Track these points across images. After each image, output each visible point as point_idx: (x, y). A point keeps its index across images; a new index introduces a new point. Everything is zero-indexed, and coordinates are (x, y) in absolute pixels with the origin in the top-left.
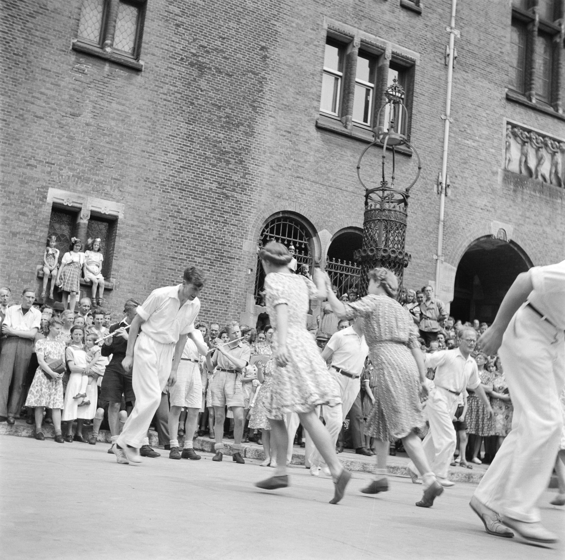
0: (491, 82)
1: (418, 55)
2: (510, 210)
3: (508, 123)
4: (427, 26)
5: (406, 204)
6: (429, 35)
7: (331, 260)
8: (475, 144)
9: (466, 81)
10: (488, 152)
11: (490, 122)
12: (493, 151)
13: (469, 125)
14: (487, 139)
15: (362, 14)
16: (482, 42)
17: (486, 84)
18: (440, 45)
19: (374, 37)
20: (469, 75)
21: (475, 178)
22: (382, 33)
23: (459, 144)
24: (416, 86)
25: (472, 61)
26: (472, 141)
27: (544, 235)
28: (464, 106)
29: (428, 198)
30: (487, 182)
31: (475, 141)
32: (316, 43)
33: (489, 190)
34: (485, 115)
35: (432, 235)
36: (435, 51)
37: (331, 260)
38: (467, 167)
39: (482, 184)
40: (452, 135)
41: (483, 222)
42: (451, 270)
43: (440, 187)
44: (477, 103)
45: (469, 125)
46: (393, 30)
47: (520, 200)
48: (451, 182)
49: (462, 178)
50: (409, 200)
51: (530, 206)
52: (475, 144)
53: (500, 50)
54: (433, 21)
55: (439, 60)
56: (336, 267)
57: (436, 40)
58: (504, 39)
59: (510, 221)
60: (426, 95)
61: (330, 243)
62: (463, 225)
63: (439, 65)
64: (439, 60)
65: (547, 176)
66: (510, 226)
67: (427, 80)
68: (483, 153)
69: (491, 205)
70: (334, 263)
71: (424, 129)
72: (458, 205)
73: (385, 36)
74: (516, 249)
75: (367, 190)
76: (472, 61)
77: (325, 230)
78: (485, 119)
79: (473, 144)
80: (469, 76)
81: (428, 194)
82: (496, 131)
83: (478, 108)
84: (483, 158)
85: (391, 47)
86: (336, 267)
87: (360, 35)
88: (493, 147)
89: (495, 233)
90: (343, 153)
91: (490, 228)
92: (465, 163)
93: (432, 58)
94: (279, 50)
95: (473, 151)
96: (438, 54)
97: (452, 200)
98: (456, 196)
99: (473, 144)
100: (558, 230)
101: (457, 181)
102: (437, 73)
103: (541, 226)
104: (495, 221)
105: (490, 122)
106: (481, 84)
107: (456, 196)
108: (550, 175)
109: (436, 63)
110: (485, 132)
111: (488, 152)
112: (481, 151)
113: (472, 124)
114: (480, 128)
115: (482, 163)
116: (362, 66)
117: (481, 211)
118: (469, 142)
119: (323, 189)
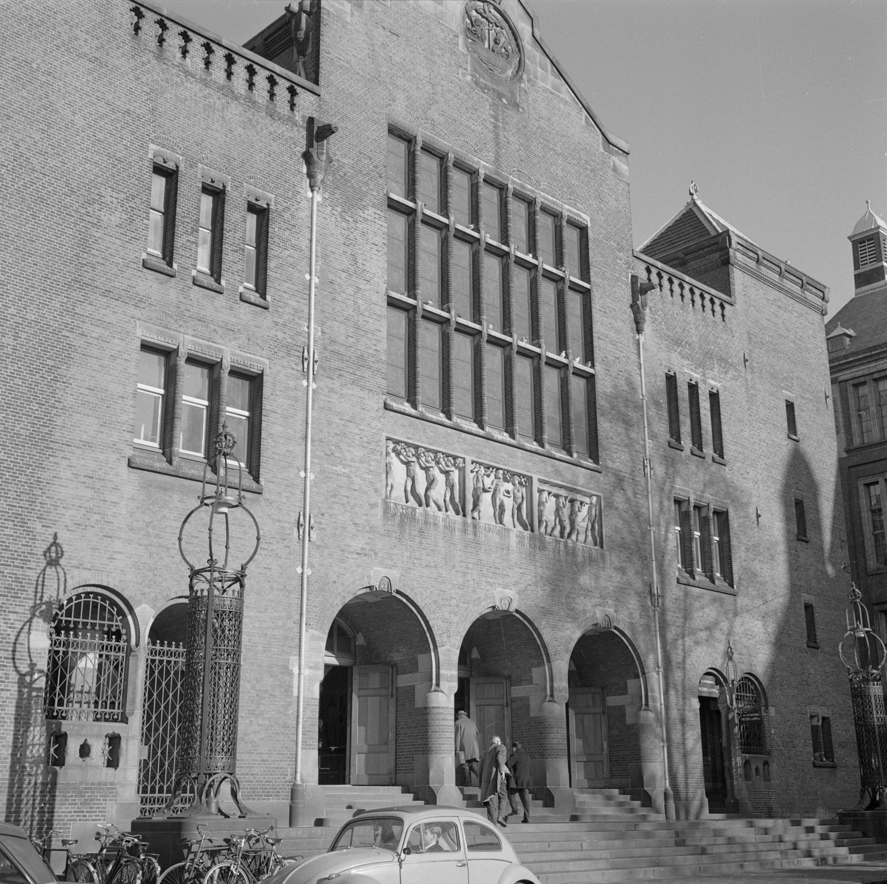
0: (363, 388)
1: (267, 361)
2: (395, 551)
3: (388, 439)
4: (276, 324)
5: (242, 586)
6: (280, 335)
7: (154, 644)
8: (346, 471)
9: (332, 390)
10: (363, 479)
11: (365, 439)
12: (370, 477)
13: (337, 446)
15: (188, 314)
17: (357, 392)
18: (295, 348)
19: (207, 343)
20: (335, 382)
21: (348, 514)
22: (217, 338)
23: (324, 472)
24: (264, 402)
25: (337, 364)
26: (341, 467)
28: (330, 423)
29: (286, 546)
30: (364, 518)
31: (345, 466)
32: (126, 356)
33: (367, 529)
34: (358, 432)
35: (292, 596)
36: (289, 355)
37: (154, 644)
38: (337, 500)
39: (357, 521)
40: (316, 461)
41: (360, 570)
42: (320, 638)
43: (301, 530)
44: (346, 418)
45: (337, 446)
46: (231, 333)
47: (407, 537)
48: (315, 522)
49: (331, 516)
50: (246, 581)
51: (421, 543)
52: (346, 471)
53: (374, 347)
54: (286, 317)
55: (294, 366)
56: (161, 653)
57: (290, 341)
58: (379, 334)
60: (279, 411)
61: (152, 621)
62: (333, 577)
63: (295, 372)
64: (294, 366)
65: (442, 504)
66: (395, 572)
67: (279, 393)
68: (357, 480)
69: (368, 548)
70: (158, 647)
71: (277, 457)
72: (326, 551)
73: (220, 341)
74: (404, 600)
75: (192, 568)
76: (337, 364)
77: (144, 605)
78: (358, 437)
79: (343, 470)
80: (336, 384)
81: (286, 543)
82: (373, 452)
84: (357, 488)
85: (230, 354)
86: (161, 653)
87: (187, 342)
88: (370, 472)
90: (167, 498)
91: (369, 577)
92: (334, 496)
93: (285, 364)
94: (73, 369)
95: (345, 479)
96: (294, 359)
97: (318, 547)
98: (323, 540)
99: (343, 470)
100: (457, 571)
101: (324, 521)
102: (292, 383)
103: (436, 567)
104: (375, 568)
105: (365, 439)
107: (323, 540)
108: (445, 501)
109: (290, 371)
110: (358, 453)
111: (363, 479)
112: (355, 479)
113: (341, 444)
114: (351, 449)
115: (356, 494)
116: (192, 380)
117: (356, 556)
118: (339, 469)
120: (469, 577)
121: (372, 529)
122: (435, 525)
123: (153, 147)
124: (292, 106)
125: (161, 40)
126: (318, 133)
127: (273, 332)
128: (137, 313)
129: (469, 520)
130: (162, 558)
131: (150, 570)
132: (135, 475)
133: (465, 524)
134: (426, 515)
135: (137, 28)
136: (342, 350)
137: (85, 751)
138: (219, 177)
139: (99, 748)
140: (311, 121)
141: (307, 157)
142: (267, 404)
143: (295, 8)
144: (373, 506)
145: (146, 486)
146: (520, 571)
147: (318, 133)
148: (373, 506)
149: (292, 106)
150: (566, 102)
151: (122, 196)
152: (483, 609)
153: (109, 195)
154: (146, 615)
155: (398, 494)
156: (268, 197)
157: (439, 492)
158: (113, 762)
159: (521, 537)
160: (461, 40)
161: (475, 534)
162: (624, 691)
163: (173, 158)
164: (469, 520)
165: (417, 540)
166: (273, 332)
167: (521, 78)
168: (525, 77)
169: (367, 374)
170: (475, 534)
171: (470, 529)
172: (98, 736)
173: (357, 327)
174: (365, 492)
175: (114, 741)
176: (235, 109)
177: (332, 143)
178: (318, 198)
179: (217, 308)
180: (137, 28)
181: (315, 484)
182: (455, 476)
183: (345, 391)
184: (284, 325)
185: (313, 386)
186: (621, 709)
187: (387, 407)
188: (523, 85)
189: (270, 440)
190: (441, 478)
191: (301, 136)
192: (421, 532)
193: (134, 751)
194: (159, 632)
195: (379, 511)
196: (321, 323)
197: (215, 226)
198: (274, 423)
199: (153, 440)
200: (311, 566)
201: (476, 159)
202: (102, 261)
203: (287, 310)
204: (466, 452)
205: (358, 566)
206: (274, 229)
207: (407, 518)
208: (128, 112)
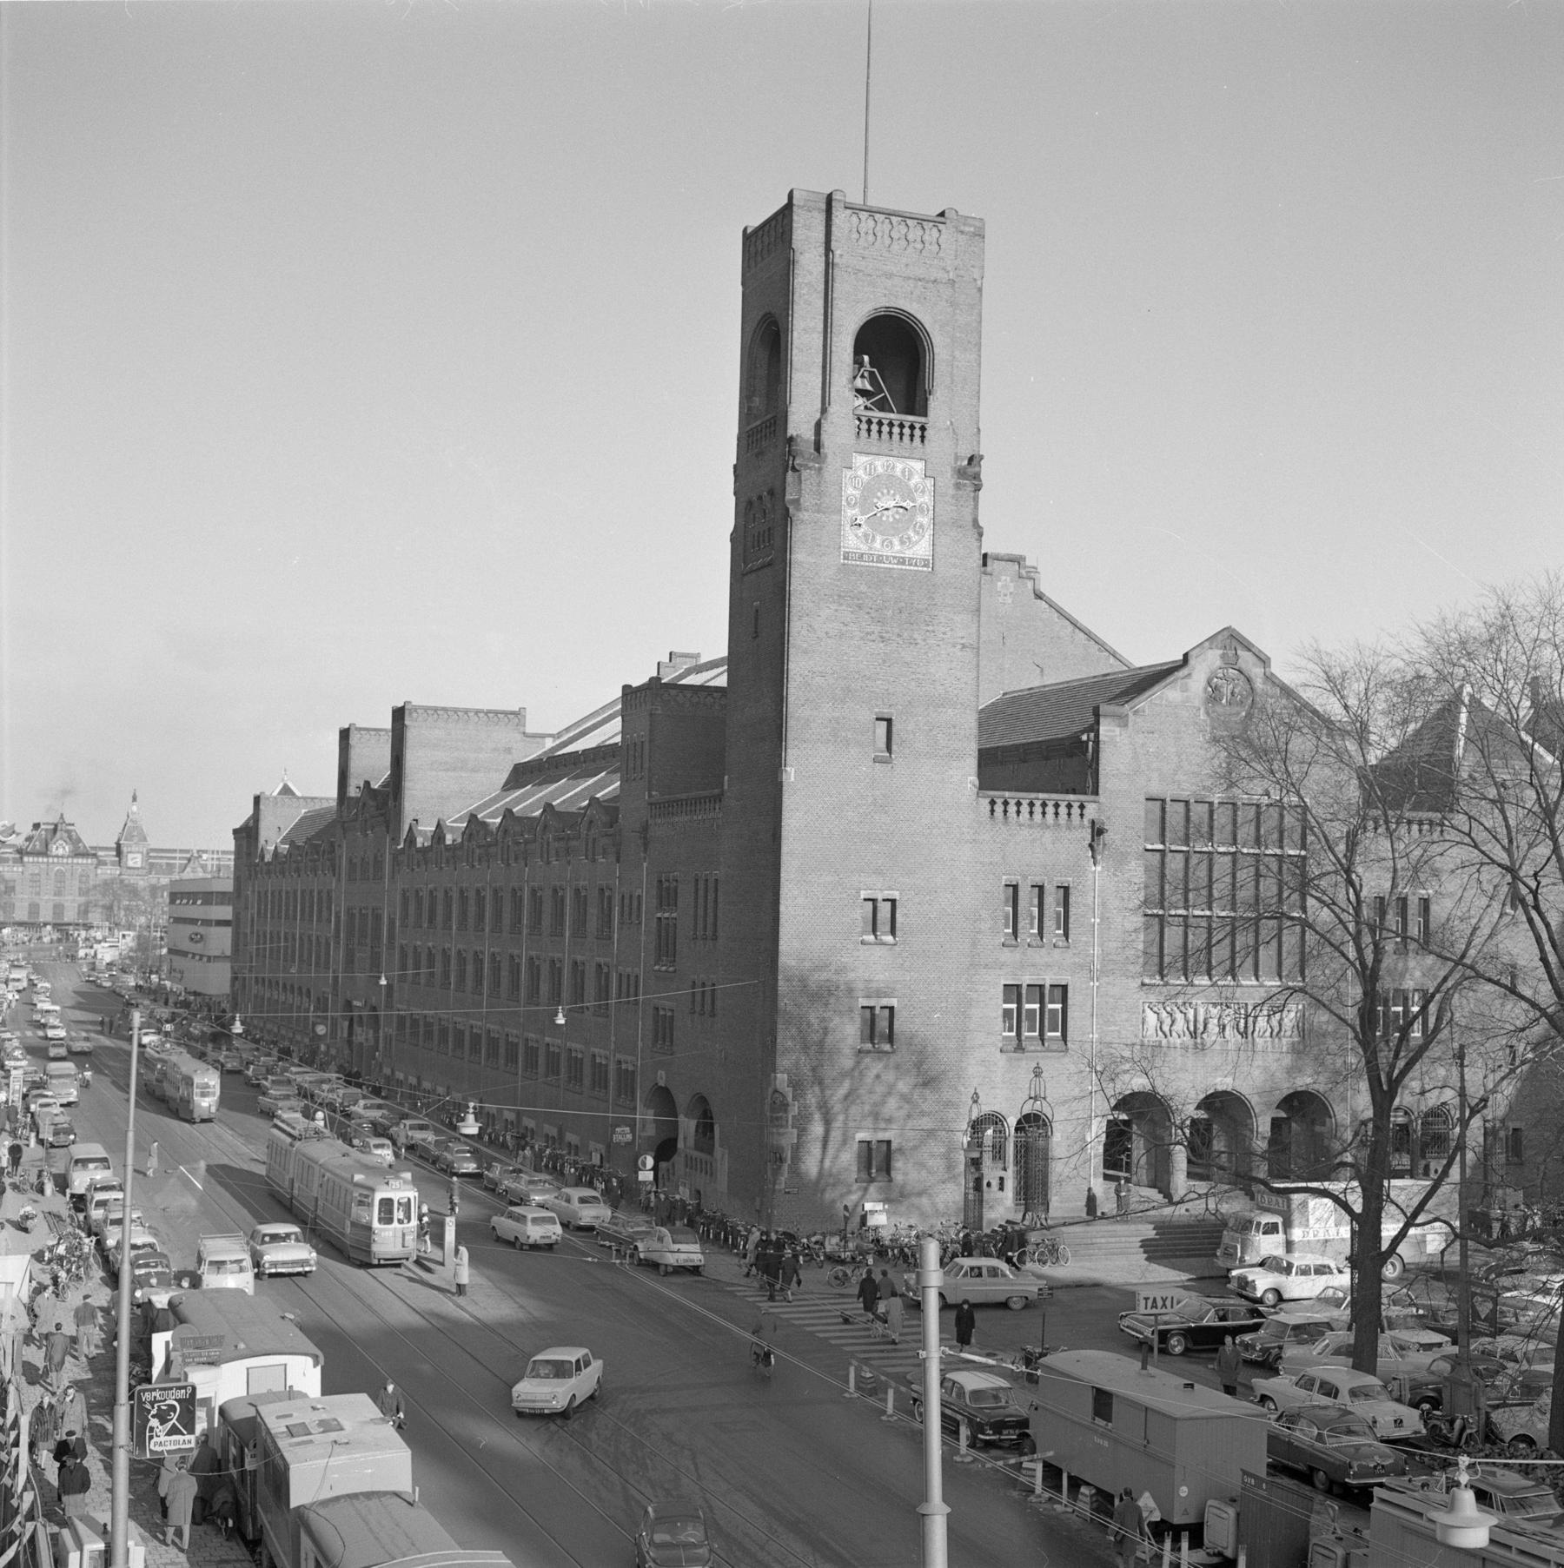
87: (1026, 980)
124: (1082, 815)
125: (1005, 812)
126: (1098, 831)
132: (1004, 1056)
135: (992, 811)
137: (989, 1185)
138: (1038, 880)
139: (995, 1183)
140: (1093, 822)
141: (1091, 846)
142: (1070, 1002)
143: (1084, 738)
145: (1009, 1060)
147: (1098, 831)
149: (1082, 815)
153: (984, 914)
154: (1012, 1121)
155: (1151, 1031)
156: (1069, 880)
157: (1180, 1025)
158: (1001, 1189)
162: (1324, 1124)
163: (1014, 880)
175: (1002, 1179)
176: (1048, 835)
177: (1106, 837)
178: (1099, 868)
179: (1040, 956)
180: (992, 811)
182: (1191, 1013)
186: (1321, 1134)
187: (1143, 984)
190: (1179, 1016)
191: (1087, 834)
193: (1010, 1184)
194: (1017, 1130)
196: (1101, 945)
197: (1039, 908)
199: (1011, 1030)
206: (1072, 899)
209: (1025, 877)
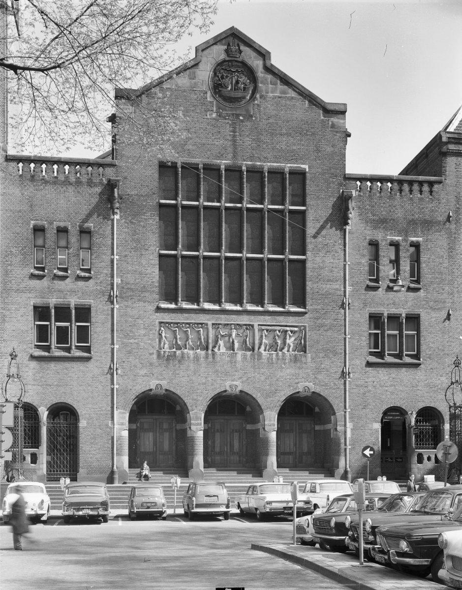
0: (145, 302)
2: (164, 372)
4: (97, 283)
8: (136, 341)
9: (127, 306)
12: (150, 341)
14: (144, 335)
15: (53, 290)
16: (137, 280)
17: (141, 304)
25: (131, 293)
27: (191, 382)
31: (135, 339)
44: (136, 317)
49: (128, 362)
52: (136, 341)
54: (101, 279)
59: (164, 378)
62: (130, 387)
76: (131, 293)
80: (130, 303)
83: (137, 320)
88: (150, 339)
89: (153, 387)
91: (149, 385)
94: (6, 324)
105: (147, 325)
106: (138, 305)
110: (143, 332)
112: (141, 344)
119: (39, 387)
120: (209, 379)
121: (151, 364)
122: (188, 357)
123: (32, 222)
127: (95, 287)
128: (30, 295)
129: (210, 352)
130: (48, 389)
131: (43, 394)
133: (207, 354)
134: (183, 354)
136: (133, 287)
144: (151, 354)
146: (243, 372)
148: (151, 354)
150: (292, 98)
151: (21, 248)
152: (212, 394)
159: (244, 357)
160: (209, 94)
161: (214, 358)
164: (210, 352)
165: (178, 365)
166: (95, 287)
167: (255, 97)
168: (258, 96)
169: (147, 294)
170: (214, 358)
171: (210, 357)
172: (28, 454)
173: (141, 273)
174: (146, 349)
181: (119, 350)
183: (135, 305)
184: (101, 283)
185: (117, 306)
188: (256, 102)
189: (95, 335)
192: (180, 361)
195: (155, 356)
198: (97, 327)
200: (118, 384)
201: (219, 161)
202: (14, 278)
203: (102, 275)
204: (208, 320)
205: (143, 381)
207: (171, 357)
208: (20, 211)
209: (51, 223)
